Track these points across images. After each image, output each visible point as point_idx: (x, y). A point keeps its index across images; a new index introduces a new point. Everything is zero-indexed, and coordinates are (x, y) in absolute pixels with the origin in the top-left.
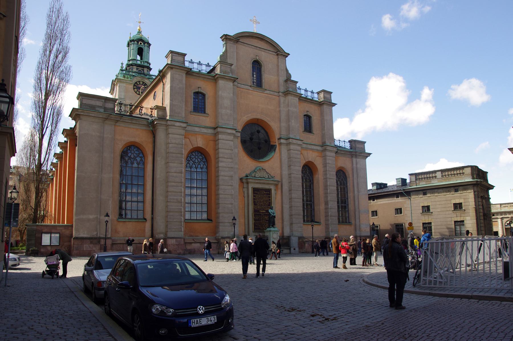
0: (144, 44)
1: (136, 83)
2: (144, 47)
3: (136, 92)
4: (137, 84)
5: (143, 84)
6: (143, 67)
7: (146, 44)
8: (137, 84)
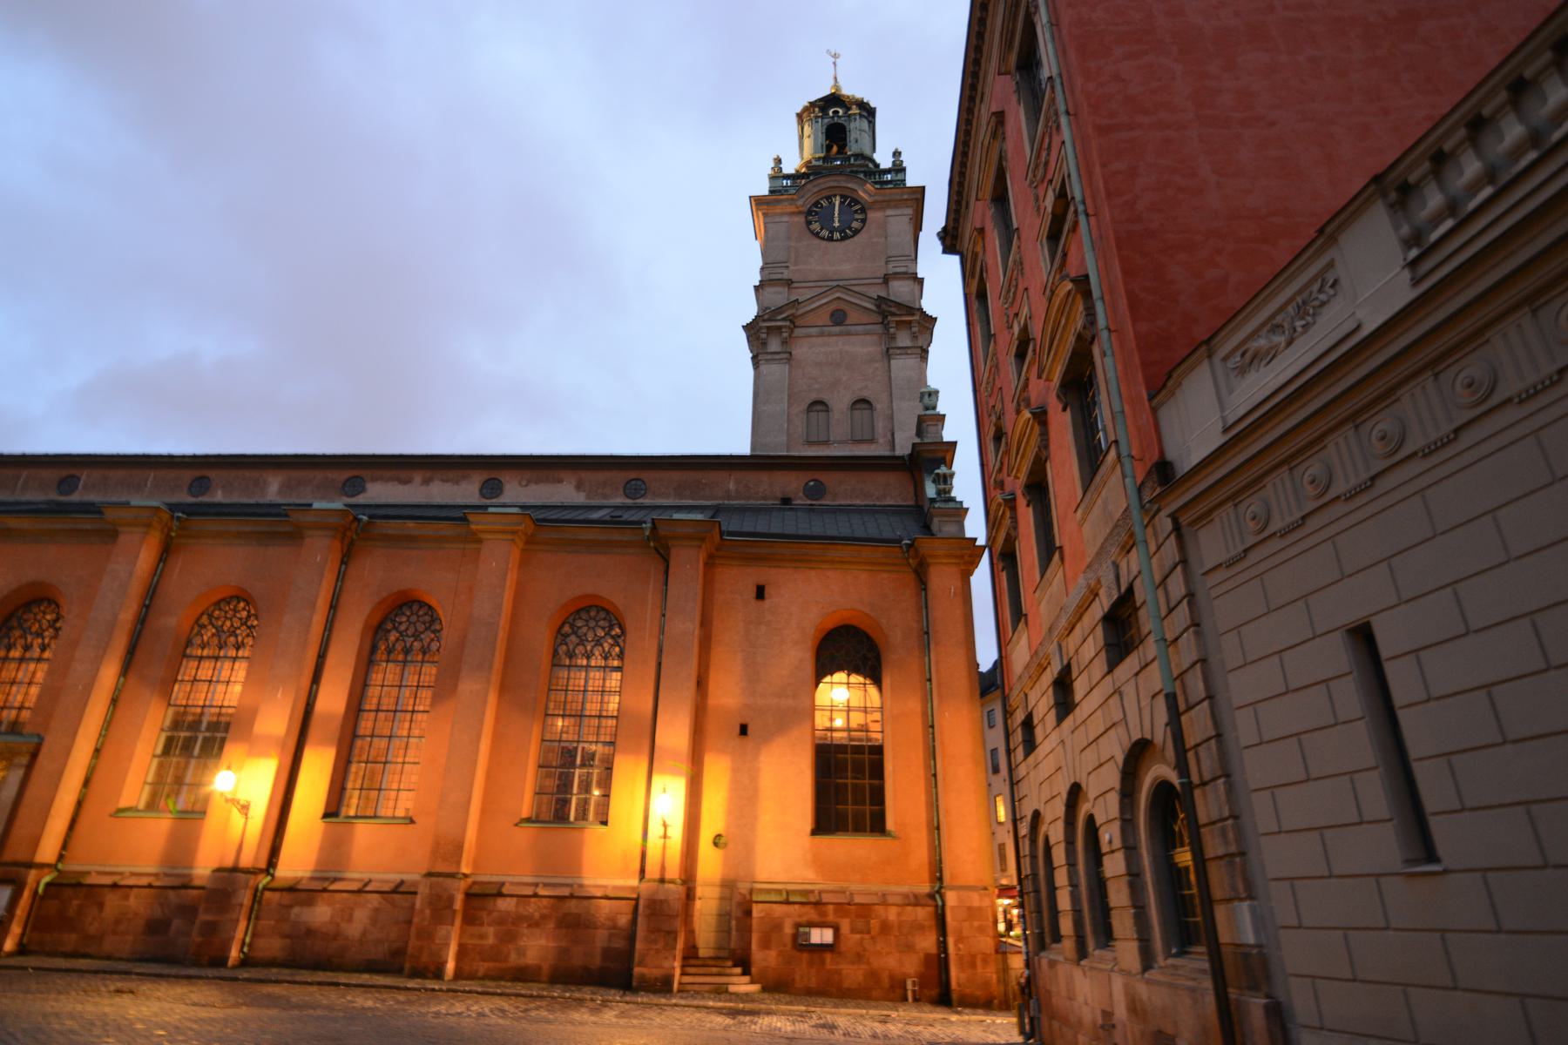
3: (817, 235)
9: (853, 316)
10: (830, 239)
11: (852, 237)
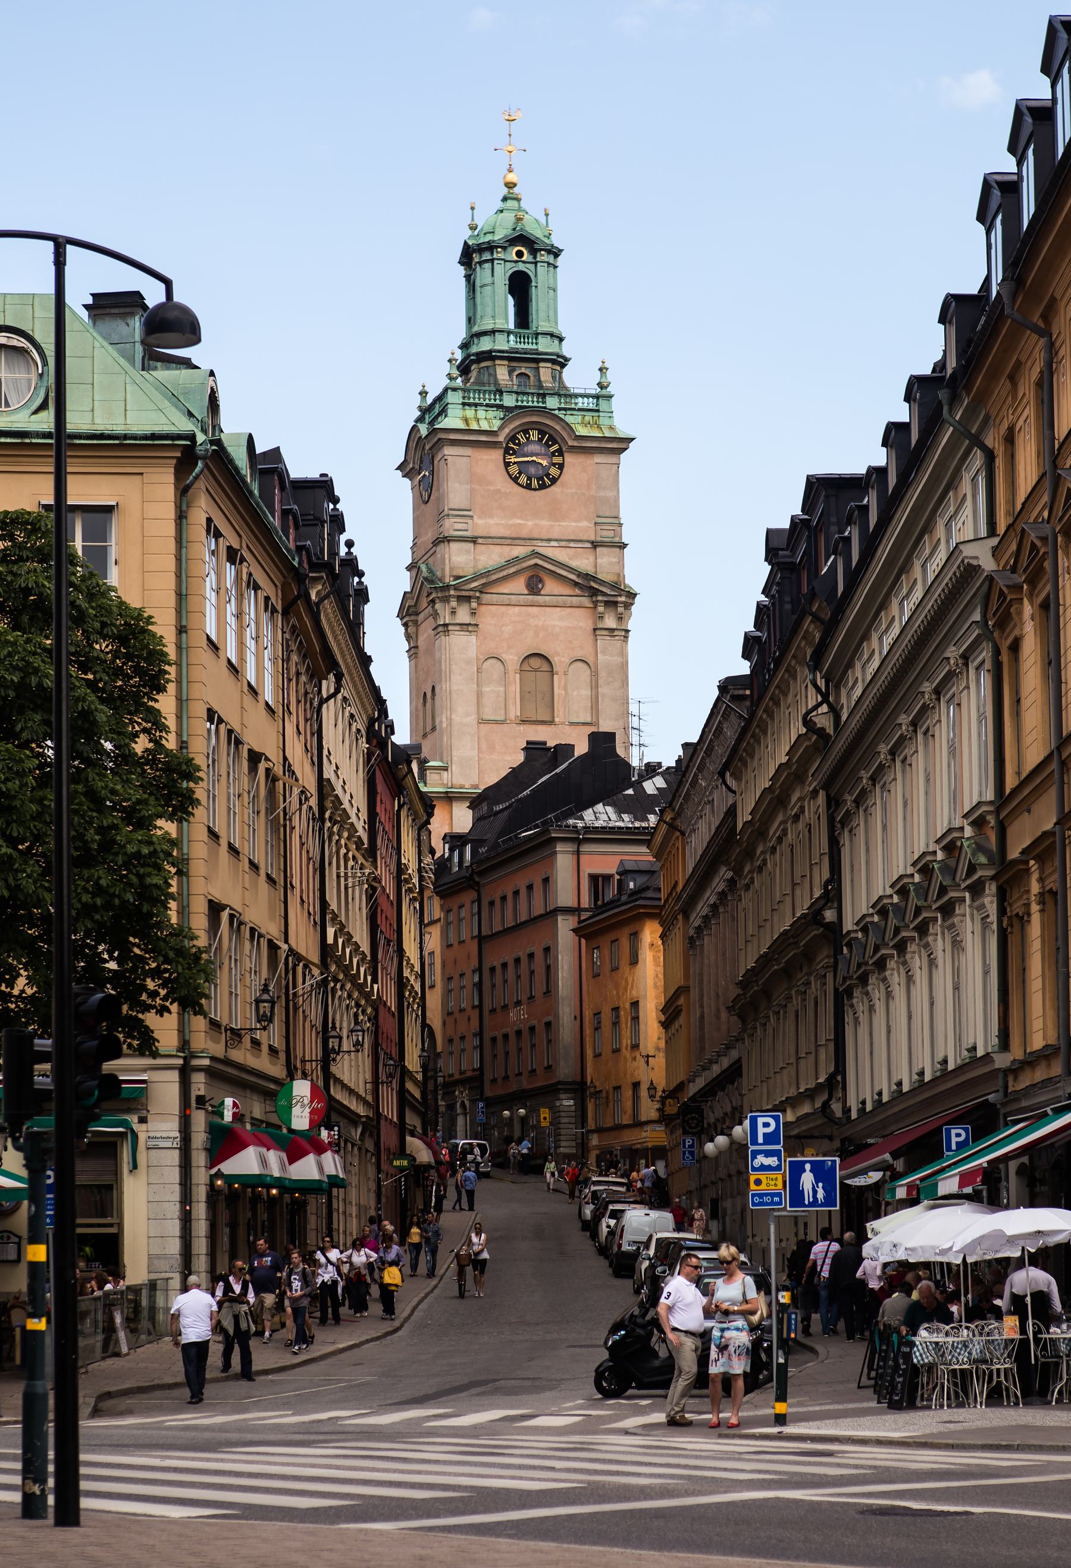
0: (534, 252)
1: (513, 438)
2: (532, 266)
3: (515, 480)
4: (519, 444)
5: (540, 440)
6: (535, 359)
7: (543, 256)
8: (519, 444)
9: (551, 586)
10: (528, 487)
11: (550, 486)
